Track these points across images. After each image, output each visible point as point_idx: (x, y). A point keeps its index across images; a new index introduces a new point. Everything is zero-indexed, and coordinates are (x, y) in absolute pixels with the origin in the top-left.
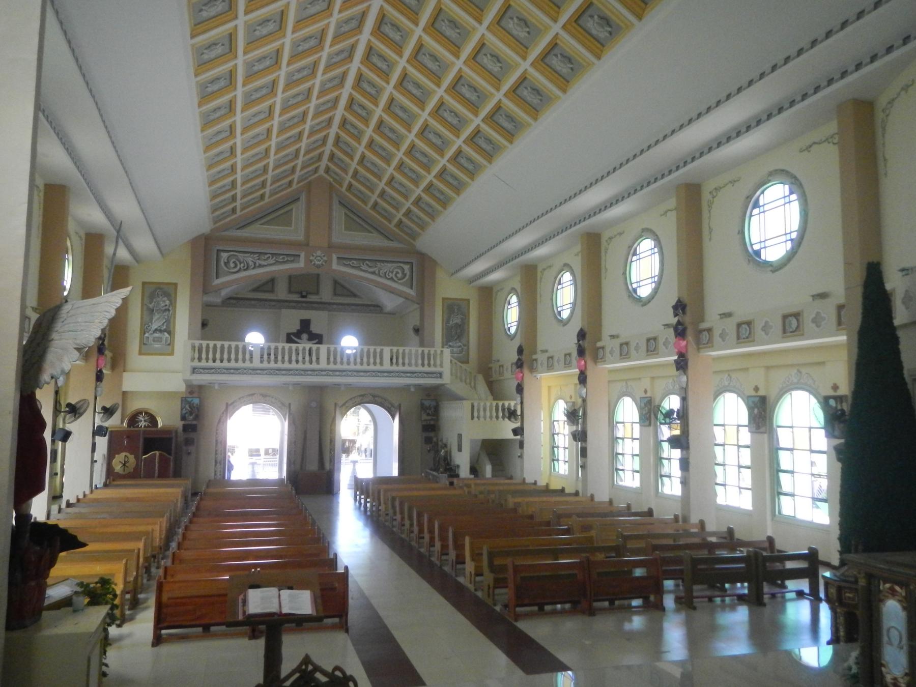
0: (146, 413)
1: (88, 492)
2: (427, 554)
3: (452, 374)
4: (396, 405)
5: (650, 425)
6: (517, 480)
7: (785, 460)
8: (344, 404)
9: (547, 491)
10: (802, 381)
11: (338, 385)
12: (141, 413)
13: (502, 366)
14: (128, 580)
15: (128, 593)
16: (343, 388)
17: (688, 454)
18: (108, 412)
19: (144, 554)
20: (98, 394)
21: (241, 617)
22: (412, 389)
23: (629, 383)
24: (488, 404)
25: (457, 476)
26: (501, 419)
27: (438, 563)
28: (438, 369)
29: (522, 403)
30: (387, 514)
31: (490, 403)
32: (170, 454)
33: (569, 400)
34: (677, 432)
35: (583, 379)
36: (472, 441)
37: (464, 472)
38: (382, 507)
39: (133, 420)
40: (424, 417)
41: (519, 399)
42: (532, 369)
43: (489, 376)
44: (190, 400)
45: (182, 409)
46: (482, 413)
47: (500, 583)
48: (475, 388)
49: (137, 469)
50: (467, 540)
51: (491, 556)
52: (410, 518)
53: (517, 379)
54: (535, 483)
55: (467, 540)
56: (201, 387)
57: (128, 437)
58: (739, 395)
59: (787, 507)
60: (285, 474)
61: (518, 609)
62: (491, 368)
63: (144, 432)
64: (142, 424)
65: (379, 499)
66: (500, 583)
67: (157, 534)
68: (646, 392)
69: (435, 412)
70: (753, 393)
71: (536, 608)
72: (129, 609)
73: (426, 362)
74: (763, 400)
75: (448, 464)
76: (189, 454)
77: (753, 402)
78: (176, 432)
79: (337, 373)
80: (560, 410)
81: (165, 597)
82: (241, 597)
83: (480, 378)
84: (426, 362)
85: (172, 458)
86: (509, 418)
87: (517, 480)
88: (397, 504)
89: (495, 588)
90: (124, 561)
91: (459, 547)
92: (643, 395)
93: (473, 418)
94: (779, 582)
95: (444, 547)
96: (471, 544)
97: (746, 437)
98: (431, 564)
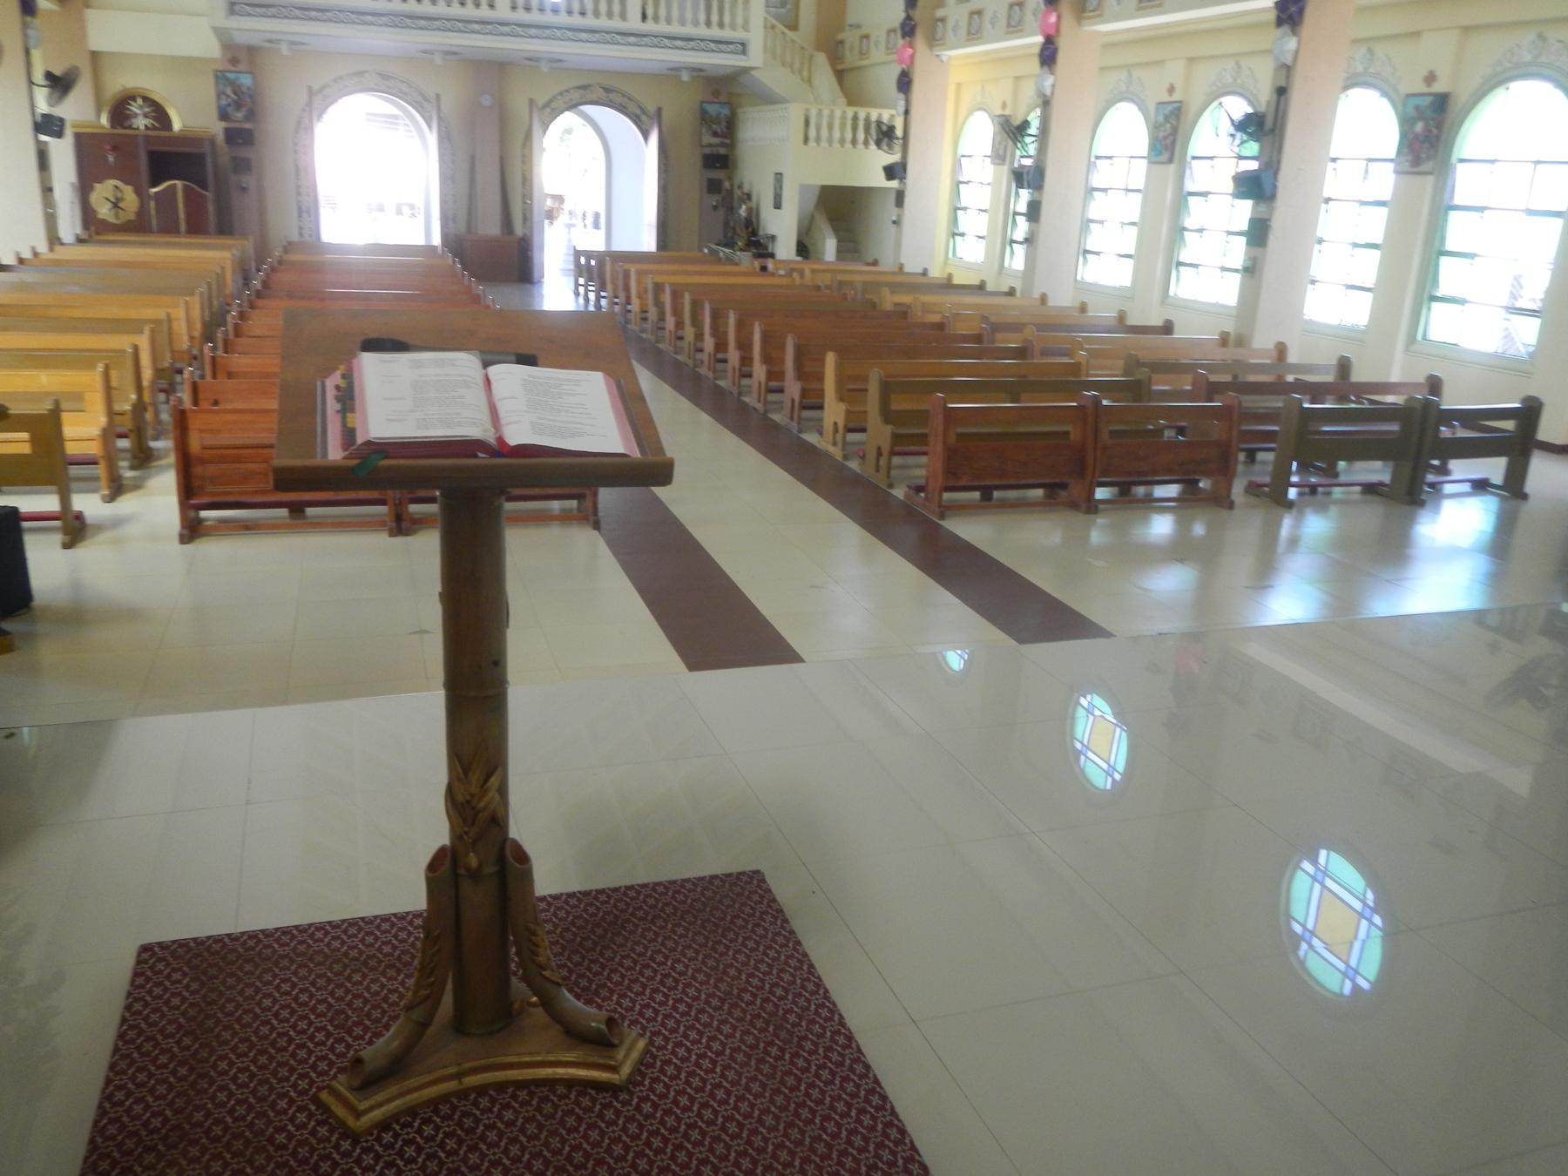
0: (146, 99)
1: (42, 247)
2: (735, 390)
3: (765, 50)
4: (652, 109)
5: (1171, 161)
6: (887, 264)
7: (1458, 231)
8: (547, 105)
9: (948, 286)
10: (1543, 59)
11: (533, 59)
12: (134, 99)
13: (867, 37)
14: (117, 407)
15: (121, 436)
16: (545, 67)
17: (1271, 210)
18: (60, 84)
19: (155, 358)
20: (32, 43)
21: (335, 453)
22: (685, 77)
23: (1136, 73)
24: (838, 113)
25: (772, 256)
26: (860, 146)
27: (759, 406)
28: (739, 35)
29: (907, 112)
30: (645, 319)
31: (843, 111)
32: (205, 187)
33: (999, 112)
34: (1253, 165)
35: (1048, 55)
36: (804, 188)
37: (785, 249)
38: (635, 306)
39: (120, 112)
40: (708, 139)
41: (902, 103)
42: (933, 41)
43: (838, 53)
46: (824, 132)
47: (907, 442)
48: (809, 81)
49: (142, 212)
50: (831, 359)
51: (887, 389)
52: (697, 322)
53: (901, 61)
54: (925, 273)
55: (831, 359)
56: (252, 51)
57: (115, 148)
58: (1385, 94)
59: (1442, 325)
60: (437, 240)
61: (946, 496)
62: (842, 42)
63: (147, 137)
64: (141, 123)
65: (627, 289)
66: (907, 442)
67: (181, 327)
68: (1171, 90)
69: (728, 129)
70: (1422, 88)
71: (976, 495)
72: (132, 468)
73: (715, 18)
74: (1442, 102)
75: (754, 233)
77: (1417, 108)
78: (212, 141)
79: (533, 31)
80: (980, 133)
81: (195, 444)
82: (334, 380)
83: (821, 59)
84: (715, 18)
85: (209, 195)
86: (878, 144)
87: (887, 264)
88: (667, 298)
89: (893, 453)
90: (100, 368)
91: (809, 375)
92: (1166, 98)
93: (806, 140)
94: (1436, 462)
95: (775, 374)
96: (839, 368)
97: (1384, 181)
98: (744, 409)
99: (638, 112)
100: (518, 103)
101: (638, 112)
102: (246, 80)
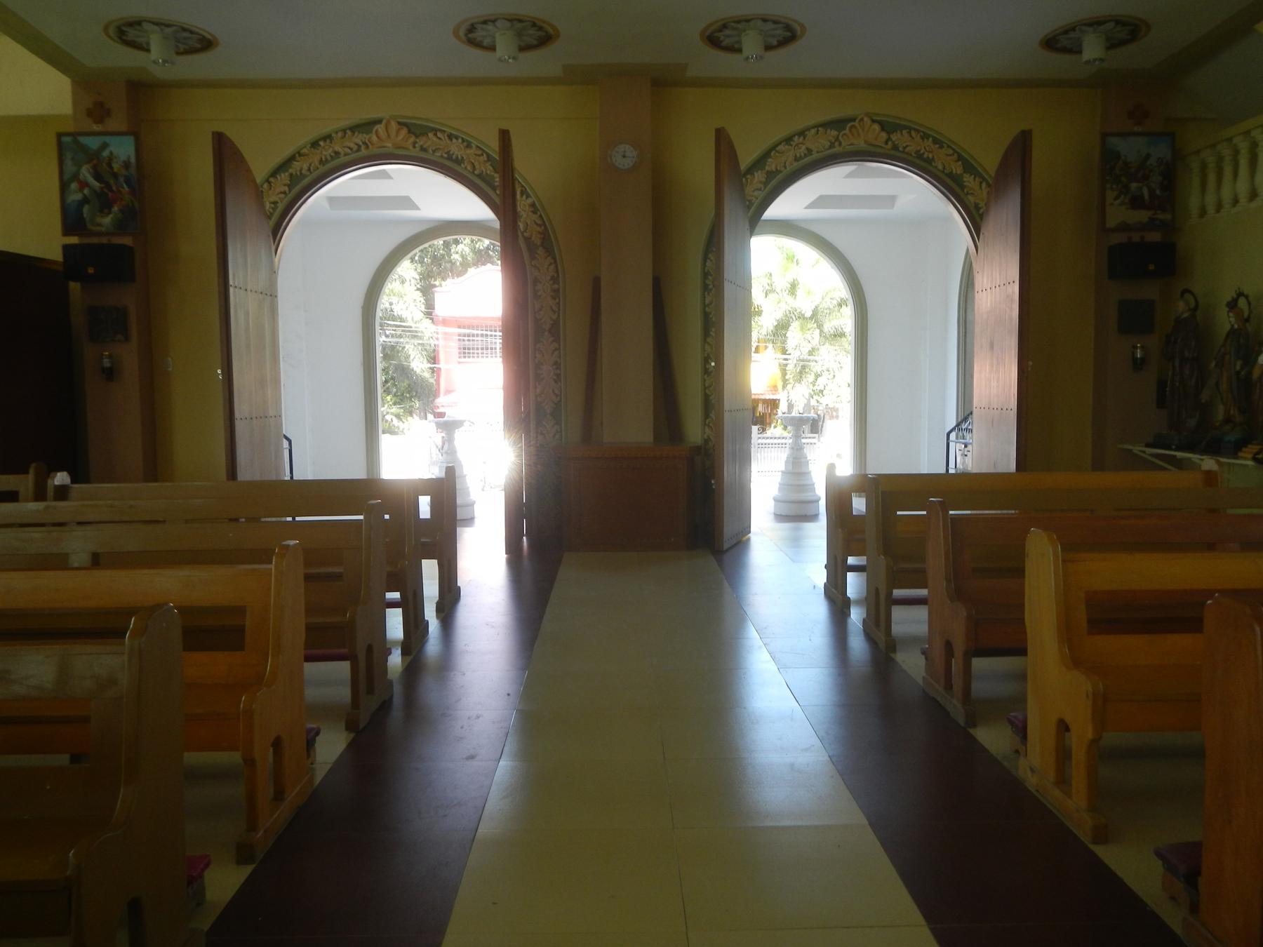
8: (759, 163)
40: (1118, 213)
44: (93, 143)
45: (64, 187)
76: (110, 374)
99: (957, 169)
100: (695, 164)
101: (957, 169)
102: (123, 149)
